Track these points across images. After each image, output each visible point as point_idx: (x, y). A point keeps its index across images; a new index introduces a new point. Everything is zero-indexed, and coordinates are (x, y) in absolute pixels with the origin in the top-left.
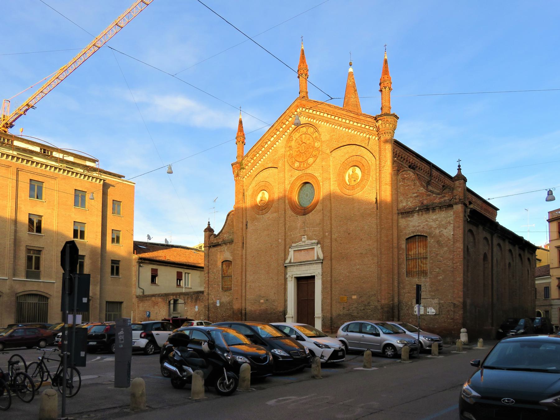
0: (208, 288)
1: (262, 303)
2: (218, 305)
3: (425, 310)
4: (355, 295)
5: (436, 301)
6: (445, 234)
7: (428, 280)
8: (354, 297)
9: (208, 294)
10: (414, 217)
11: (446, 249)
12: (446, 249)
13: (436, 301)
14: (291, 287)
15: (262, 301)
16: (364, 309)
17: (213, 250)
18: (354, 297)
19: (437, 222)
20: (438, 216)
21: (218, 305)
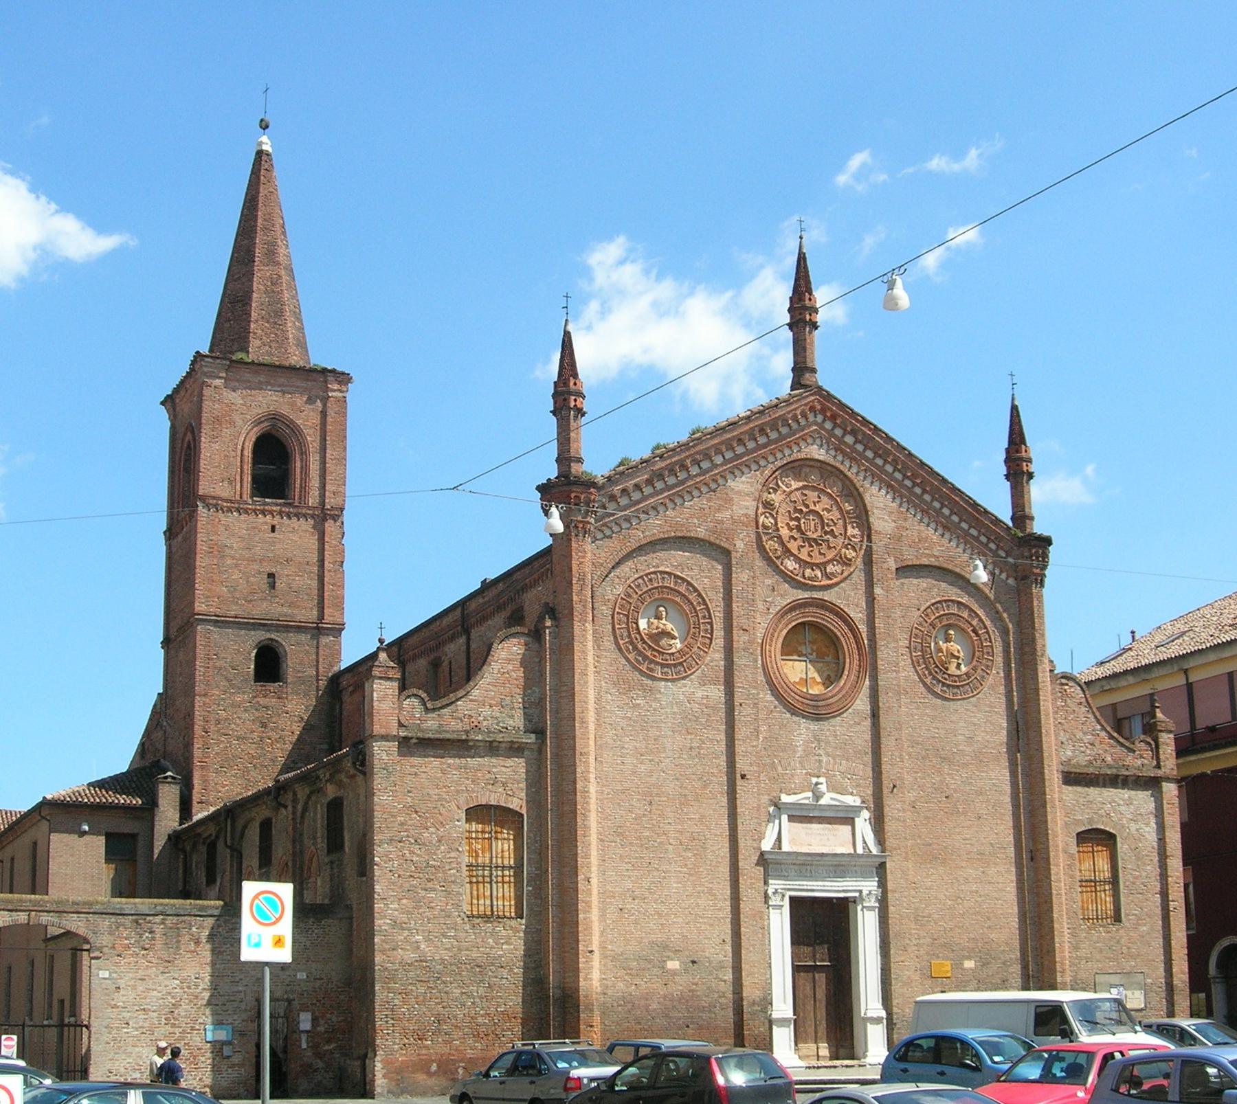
1: (674, 973)
4: (969, 958)
14: (780, 924)
15: (673, 965)
18: (969, 964)
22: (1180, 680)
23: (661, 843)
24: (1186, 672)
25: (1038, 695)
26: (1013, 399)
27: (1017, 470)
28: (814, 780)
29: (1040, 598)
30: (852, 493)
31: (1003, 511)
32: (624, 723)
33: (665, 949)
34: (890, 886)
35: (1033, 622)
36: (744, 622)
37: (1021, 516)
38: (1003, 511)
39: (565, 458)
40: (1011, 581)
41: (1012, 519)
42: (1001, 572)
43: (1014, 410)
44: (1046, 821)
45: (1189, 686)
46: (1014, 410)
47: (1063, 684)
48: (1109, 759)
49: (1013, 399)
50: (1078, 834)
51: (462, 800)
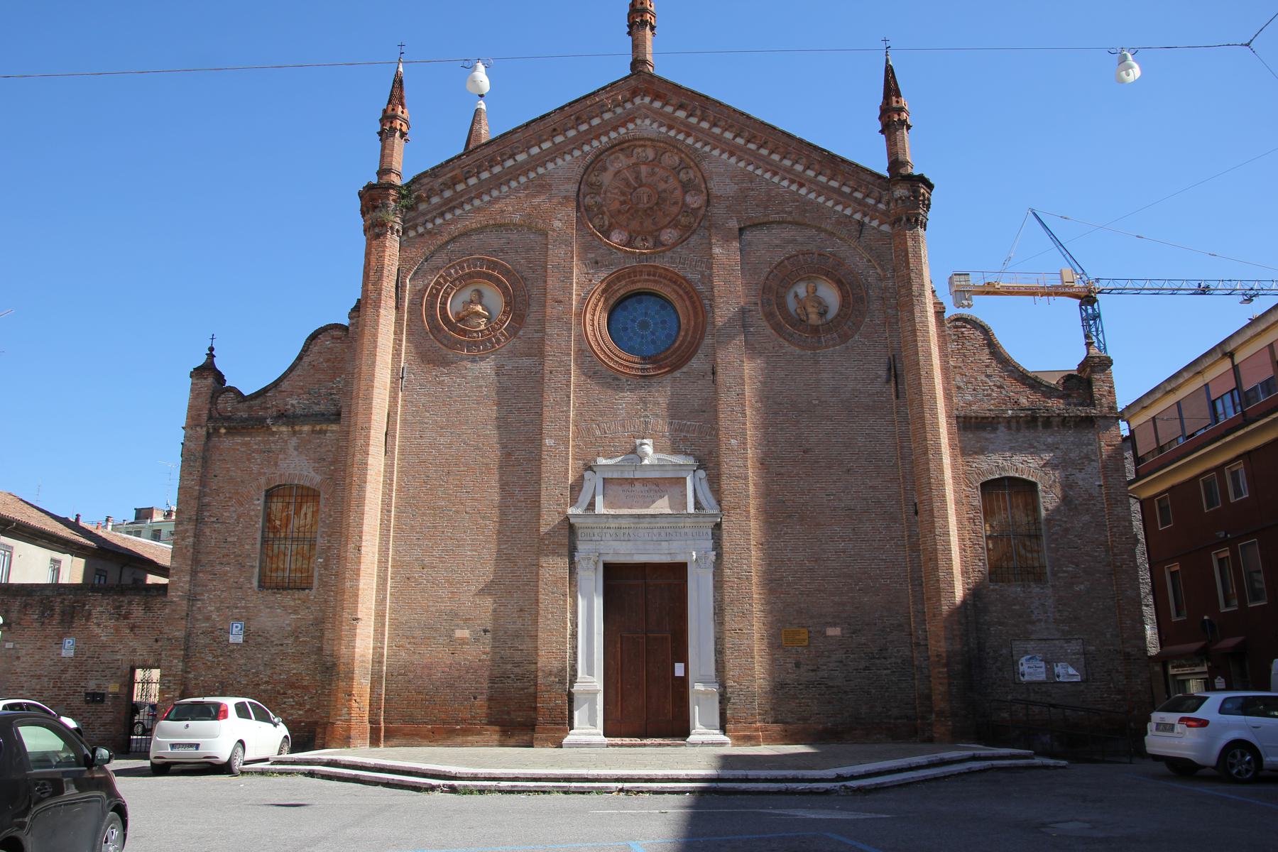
0: (194, 573)
1: (463, 642)
2: (236, 637)
3: (1050, 671)
4: (835, 625)
5: (1075, 646)
6: (1080, 483)
7: (1049, 591)
8: (833, 632)
9: (192, 598)
10: (999, 433)
11: (1087, 518)
12: (1087, 518)
13: (1075, 646)
16: (866, 668)
17: (228, 443)
18: (833, 632)
19: (1059, 453)
20: (1058, 438)
21: (236, 637)
22: (1226, 365)
23: (457, 512)
24: (1231, 355)
25: (915, 336)
26: (887, 61)
27: (892, 120)
28: (638, 442)
29: (916, 239)
30: (691, 160)
31: (880, 166)
32: (423, 399)
33: (453, 616)
34: (726, 545)
35: (908, 263)
36: (559, 295)
37: (896, 164)
38: (880, 166)
39: (384, 171)
40: (885, 228)
41: (889, 170)
42: (872, 219)
43: (889, 72)
44: (928, 469)
45: (1235, 368)
46: (889, 72)
47: (956, 327)
48: (1023, 401)
49: (887, 61)
50: (984, 485)
51: (263, 480)
